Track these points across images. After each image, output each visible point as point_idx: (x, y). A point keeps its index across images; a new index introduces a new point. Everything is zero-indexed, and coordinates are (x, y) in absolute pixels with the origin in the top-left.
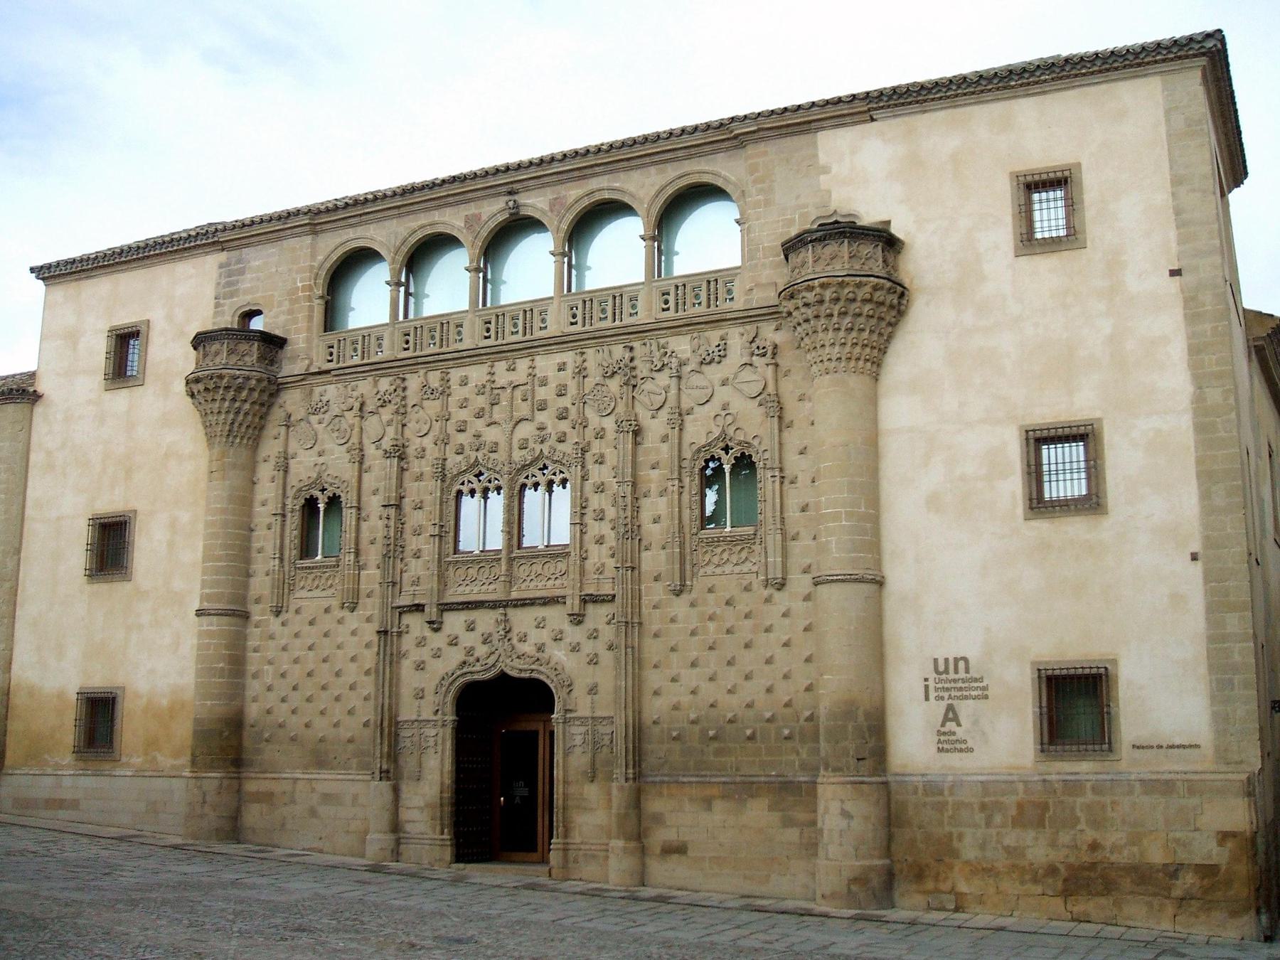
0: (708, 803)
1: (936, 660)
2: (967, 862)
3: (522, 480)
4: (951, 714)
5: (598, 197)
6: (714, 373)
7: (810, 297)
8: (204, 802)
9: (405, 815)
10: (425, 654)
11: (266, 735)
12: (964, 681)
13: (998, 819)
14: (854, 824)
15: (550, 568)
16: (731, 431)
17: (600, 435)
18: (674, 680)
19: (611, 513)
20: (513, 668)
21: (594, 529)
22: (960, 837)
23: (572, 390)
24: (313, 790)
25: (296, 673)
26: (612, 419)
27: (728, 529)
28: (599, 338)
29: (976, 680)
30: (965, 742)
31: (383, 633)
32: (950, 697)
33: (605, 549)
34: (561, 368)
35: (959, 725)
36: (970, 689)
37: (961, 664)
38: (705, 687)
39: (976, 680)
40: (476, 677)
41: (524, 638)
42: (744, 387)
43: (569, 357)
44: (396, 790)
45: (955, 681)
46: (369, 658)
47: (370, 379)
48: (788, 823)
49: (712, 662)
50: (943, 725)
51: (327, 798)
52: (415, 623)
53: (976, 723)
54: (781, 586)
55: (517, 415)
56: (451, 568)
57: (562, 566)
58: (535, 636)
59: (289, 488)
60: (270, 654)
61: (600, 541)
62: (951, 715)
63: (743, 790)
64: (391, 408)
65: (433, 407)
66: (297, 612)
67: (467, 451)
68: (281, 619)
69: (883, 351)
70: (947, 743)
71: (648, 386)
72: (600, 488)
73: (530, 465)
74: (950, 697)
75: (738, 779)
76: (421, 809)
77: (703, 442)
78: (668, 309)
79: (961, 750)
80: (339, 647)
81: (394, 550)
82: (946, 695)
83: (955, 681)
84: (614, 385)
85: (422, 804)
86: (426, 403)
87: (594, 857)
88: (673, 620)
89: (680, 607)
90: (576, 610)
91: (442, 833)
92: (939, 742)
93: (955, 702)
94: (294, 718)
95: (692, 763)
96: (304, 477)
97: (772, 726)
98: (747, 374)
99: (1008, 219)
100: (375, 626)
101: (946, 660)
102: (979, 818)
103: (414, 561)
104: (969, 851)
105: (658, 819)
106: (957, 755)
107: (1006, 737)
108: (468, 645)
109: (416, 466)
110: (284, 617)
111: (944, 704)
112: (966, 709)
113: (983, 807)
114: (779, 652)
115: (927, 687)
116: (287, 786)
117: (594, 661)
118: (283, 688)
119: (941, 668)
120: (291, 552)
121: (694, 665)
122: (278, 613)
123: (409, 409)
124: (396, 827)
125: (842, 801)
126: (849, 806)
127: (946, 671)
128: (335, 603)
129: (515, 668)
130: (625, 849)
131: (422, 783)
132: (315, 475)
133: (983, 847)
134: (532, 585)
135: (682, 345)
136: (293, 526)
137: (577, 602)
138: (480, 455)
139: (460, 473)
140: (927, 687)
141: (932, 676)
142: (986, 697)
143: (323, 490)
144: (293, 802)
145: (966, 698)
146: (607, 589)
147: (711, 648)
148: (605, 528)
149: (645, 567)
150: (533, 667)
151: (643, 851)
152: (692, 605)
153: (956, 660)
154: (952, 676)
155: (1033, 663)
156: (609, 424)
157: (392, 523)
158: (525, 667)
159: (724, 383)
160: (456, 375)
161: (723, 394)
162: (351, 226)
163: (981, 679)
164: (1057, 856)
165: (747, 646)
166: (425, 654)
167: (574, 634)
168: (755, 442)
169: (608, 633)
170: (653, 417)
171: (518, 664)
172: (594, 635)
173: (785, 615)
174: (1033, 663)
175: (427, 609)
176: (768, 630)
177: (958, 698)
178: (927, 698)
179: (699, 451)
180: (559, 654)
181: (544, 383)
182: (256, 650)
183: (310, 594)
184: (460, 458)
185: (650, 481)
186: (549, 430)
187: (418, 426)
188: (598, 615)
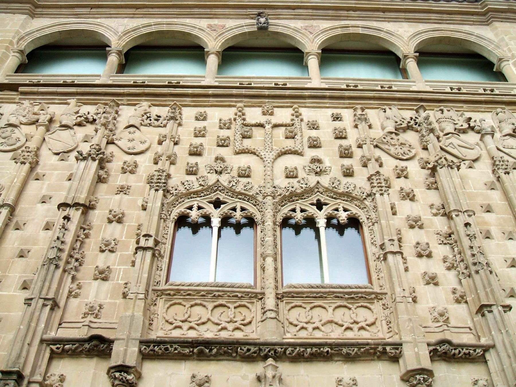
3: (285, 210)
5: (351, 30)
47: (73, 101)
55: (277, 148)
56: (161, 303)
64: (89, 129)
65: (151, 134)
71: (454, 140)
81: (66, 260)
86: (142, 128)
103: (96, 283)
109: (118, 179)
137: (425, 352)
138: (224, 179)
157: (73, 226)
160: (189, 113)
162: (77, 15)
175: (117, 348)
187: (130, 145)
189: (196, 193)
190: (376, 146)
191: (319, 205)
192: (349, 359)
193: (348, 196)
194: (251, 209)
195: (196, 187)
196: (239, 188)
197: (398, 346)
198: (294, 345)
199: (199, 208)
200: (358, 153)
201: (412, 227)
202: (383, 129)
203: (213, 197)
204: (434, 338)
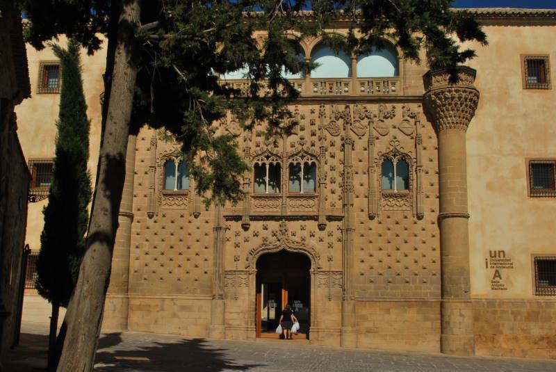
0: (388, 311)
1: (491, 252)
2: (506, 336)
3: (290, 161)
4: (497, 274)
6: (388, 121)
7: (448, 94)
8: (115, 310)
9: (228, 316)
10: (240, 239)
11: (146, 276)
12: (502, 260)
13: (519, 318)
14: (466, 320)
15: (305, 202)
16: (398, 148)
17: (332, 145)
18: (371, 256)
19: (339, 180)
20: (290, 248)
21: (330, 186)
22: (503, 325)
23: (318, 122)
24: (175, 304)
25: (163, 247)
26: (339, 137)
27: (395, 191)
28: (333, 101)
29: (508, 260)
30: (503, 286)
31: (218, 229)
32: (497, 267)
33: (336, 196)
34: (312, 112)
35: (501, 278)
36: (506, 264)
37: (502, 254)
38: (386, 259)
39: (508, 260)
40: (270, 251)
41: (294, 235)
42: (403, 129)
43: (316, 107)
44: (224, 304)
45: (498, 261)
46: (209, 240)
48: (426, 319)
49: (390, 248)
50: (494, 278)
51: (183, 308)
52: (235, 226)
53: (508, 277)
54: (420, 217)
57: (311, 202)
58: (300, 233)
59: (157, 154)
60: (147, 236)
61: (333, 192)
62: (497, 275)
63: (406, 303)
66: (164, 216)
67: (262, 145)
68: (153, 220)
69: (469, 121)
70: (496, 285)
71: (357, 124)
72: (333, 169)
73: (296, 155)
74: (497, 267)
75: (402, 300)
76: (238, 313)
77: (384, 151)
78: (379, 91)
79: (502, 289)
80: (190, 234)
82: (495, 266)
83: (499, 260)
84: (340, 122)
85: (238, 310)
87: (332, 335)
88: (370, 229)
89: (373, 224)
90: (324, 222)
91: (251, 324)
92: (493, 285)
93: (499, 269)
94: (162, 268)
95: (380, 293)
96: (167, 150)
97: (418, 277)
98: (405, 124)
99: (520, 73)
100: (212, 225)
101: (495, 252)
102: (511, 317)
104: (507, 331)
105: (364, 318)
106: (501, 291)
107: (522, 284)
108: (265, 236)
110: (155, 218)
111: (495, 269)
112: (503, 272)
113: (512, 313)
114: (420, 245)
115: (487, 263)
116: (159, 302)
117: (330, 246)
118: (156, 253)
119: (493, 255)
120: (158, 187)
121: (381, 249)
122: (151, 217)
123: (228, 123)
124: (224, 322)
125: (460, 310)
126: (463, 312)
127: (495, 256)
128: (186, 213)
129: (292, 247)
130: (352, 331)
131: (238, 301)
132: (173, 150)
133: (512, 329)
134: (297, 210)
135: (374, 108)
136: (160, 173)
137: (324, 218)
139: (257, 156)
140: (487, 263)
141: (489, 258)
142: (512, 267)
143: (177, 157)
144: (163, 310)
145: (504, 267)
146: (338, 213)
147: (389, 242)
148: (336, 187)
149: (355, 205)
150: (301, 247)
151: (357, 332)
152: (380, 223)
153: (499, 252)
154: (497, 258)
155: (532, 255)
156: (338, 141)
158: (297, 247)
159: (395, 127)
161: (393, 132)
163: (510, 260)
164: (544, 333)
165: (406, 242)
166: (240, 239)
167: (319, 233)
168: (409, 154)
169: (338, 234)
170: (360, 138)
171: (295, 246)
172: (330, 235)
173: (424, 230)
174: (532, 255)
175: (243, 218)
176: (416, 236)
177: (501, 267)
178: (487, 267)
179: (383, 155)
180: (313, 242)
181: (303, 118)
182: (138, 234)
183: (171, 207)
184: (258, 148)
185: (357, 167)
186: (306, 139)
188: (331, 226)
189: (261, 155)
190: (326, 129)
191: (302, 157)
192: (304, 220)
193: (312, 155)
194: (279, 161)
195: (260, 153)
196: (275, 153)
197: (318, 216)
198: (290, 216)
199: (262, 160)
200: (318, 133)
201: (331, 170)
202: (330, 118)
203: (266, 154)
204: (328, 214)
